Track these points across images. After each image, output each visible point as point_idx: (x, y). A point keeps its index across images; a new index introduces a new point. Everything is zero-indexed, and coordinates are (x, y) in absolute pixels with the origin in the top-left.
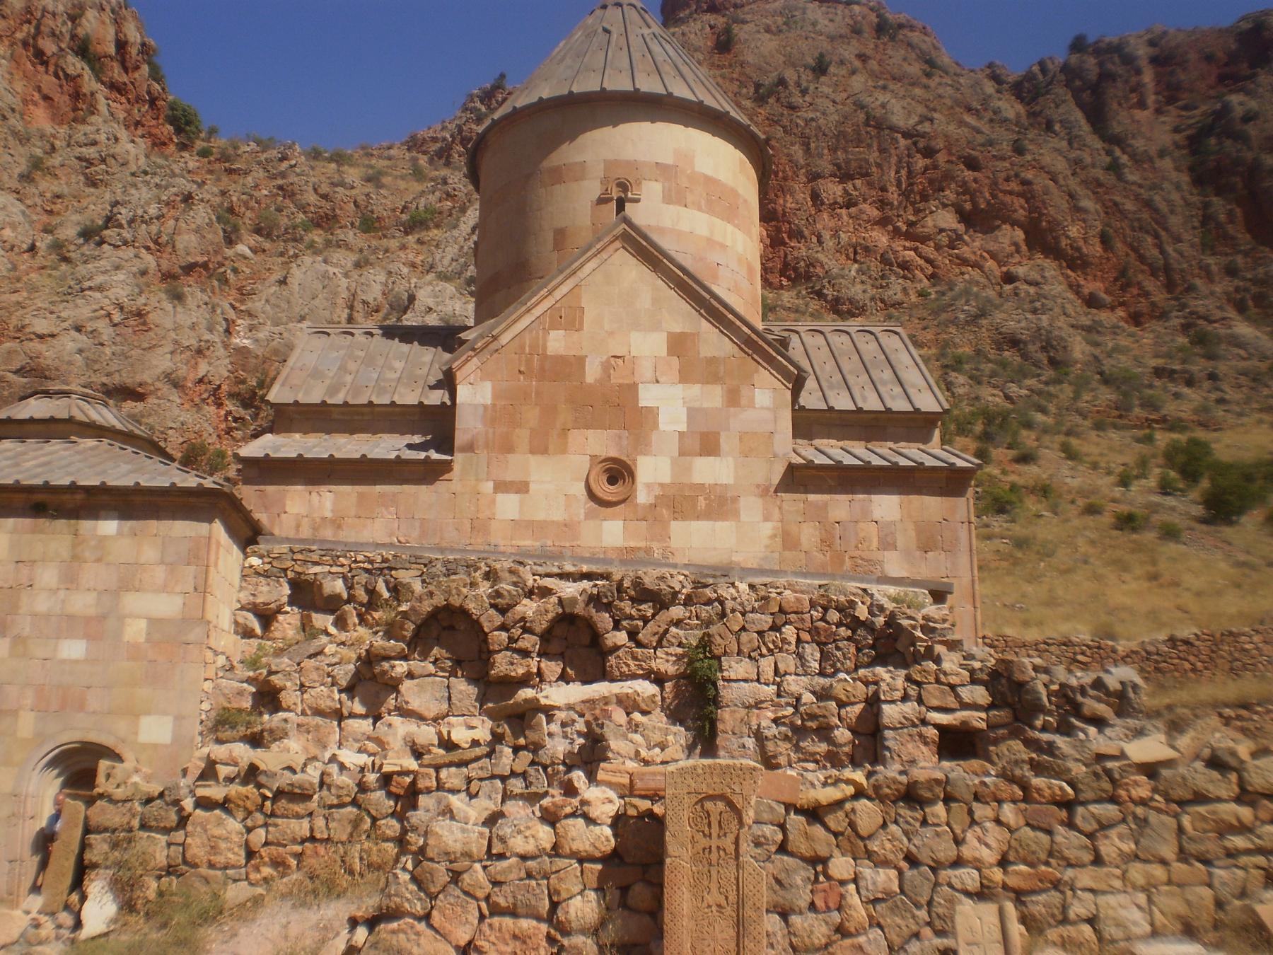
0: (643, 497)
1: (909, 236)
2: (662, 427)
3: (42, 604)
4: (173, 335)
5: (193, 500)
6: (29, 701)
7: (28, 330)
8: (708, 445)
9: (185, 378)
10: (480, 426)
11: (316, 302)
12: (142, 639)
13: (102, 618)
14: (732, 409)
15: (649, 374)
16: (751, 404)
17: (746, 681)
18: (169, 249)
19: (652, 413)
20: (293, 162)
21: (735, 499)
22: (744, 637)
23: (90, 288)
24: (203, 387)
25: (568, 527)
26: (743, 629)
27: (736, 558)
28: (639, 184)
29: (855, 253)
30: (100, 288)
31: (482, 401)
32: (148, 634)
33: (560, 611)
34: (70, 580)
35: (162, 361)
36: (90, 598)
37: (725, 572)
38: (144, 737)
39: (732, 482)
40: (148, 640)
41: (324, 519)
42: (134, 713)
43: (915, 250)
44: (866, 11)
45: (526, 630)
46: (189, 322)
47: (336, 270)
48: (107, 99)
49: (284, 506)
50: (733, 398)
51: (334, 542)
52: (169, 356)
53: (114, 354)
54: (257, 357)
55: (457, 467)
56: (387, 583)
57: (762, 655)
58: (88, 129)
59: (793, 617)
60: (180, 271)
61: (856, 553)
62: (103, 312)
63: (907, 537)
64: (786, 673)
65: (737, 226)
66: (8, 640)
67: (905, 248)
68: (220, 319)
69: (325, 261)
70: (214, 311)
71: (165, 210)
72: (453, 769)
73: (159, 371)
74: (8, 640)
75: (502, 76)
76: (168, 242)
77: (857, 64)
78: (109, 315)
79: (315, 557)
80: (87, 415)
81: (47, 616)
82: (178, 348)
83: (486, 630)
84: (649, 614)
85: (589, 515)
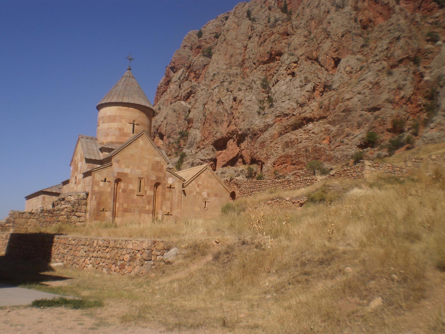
4: (388, 87)
7: (344, 99)
9: (394, 99)
18: (392, 58)
23: (362, 80)
24: (403, 100)
30: (364, 79)
35: (385, 96)
46: (393, 80)
52: (387, 94)
54: (431, 82)
58: (391, 20)
60: (397, 63)
62: (366, 86)
70: (409, 72)
71: (389, 46)
73: (384, 99)
76: (391, 56)
78: (368, 86)
82: (390, 90)
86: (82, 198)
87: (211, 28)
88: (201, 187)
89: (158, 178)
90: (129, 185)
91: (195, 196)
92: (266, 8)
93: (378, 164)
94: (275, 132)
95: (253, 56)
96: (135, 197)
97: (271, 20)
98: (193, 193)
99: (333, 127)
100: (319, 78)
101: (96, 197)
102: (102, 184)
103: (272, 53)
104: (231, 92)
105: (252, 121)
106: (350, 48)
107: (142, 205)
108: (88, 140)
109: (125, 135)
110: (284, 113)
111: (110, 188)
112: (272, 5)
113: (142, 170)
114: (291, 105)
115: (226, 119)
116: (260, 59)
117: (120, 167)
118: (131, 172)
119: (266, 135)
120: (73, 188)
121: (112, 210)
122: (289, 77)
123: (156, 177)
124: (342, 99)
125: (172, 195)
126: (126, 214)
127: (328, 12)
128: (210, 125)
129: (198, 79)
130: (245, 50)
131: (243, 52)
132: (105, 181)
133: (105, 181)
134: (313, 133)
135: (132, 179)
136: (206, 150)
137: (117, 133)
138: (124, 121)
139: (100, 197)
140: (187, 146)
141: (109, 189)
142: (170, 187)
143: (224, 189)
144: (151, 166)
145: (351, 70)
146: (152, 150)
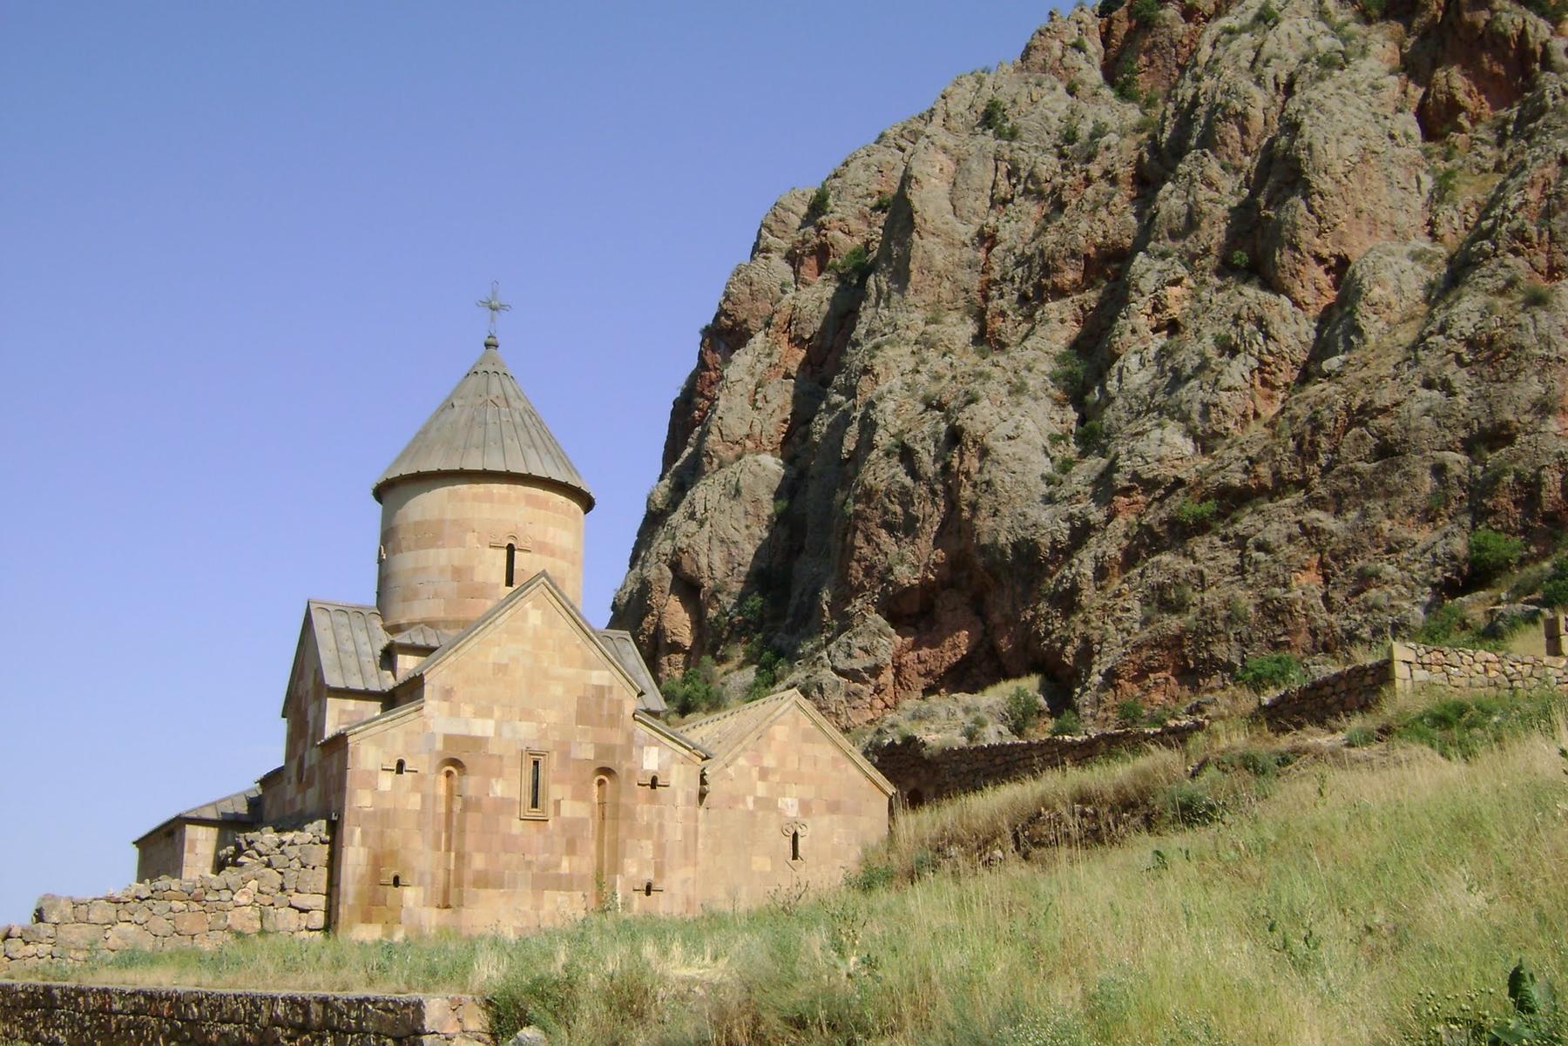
53: (1470, 399)
65: (443, 546)
78: (1459, 359)
86: (317, 840)
87: (862, 176)
88: (775, 778)
89: (604, 750)
90: (493, 781)
91: (752, 814)
92: (1061, 88)
93: (1440, 656)
94: (1113, 551)
96: (517, 827)
97: (1080, 133)
98: (744, 802)
99: (1332, 520)
100: (1267, 336)
101: (364, 834)
102: (386, 781)
103: (1087, 257)
104: (940, 407)
105: (1024, 515)
106: (1384, 216)
107: (543, 857)
108: (344, 619)
109: (479, 591)
110: (1145, 476)
111: (418, 797)
113: (541, 723)
115: (929, 509)
116: (1044, 281)
117: (454, 713)
118: (498, 733)
119: (1084, 563)
120: (292, 802)
121: (428, 879)
122: (1160, 340)
123: (596, 746)
124: (1362, 410)
125: (660, 814)
126: (483, 893)
128: (868, 540)
129: (821, 366)
130: (989, 250)
131: (981, 255)
132: (400, 766)
133: (400, 766)
134: (1261, 547)
135: (500, 757)
136: (856, 635)
137: (449, 586)
138: (471, 539)
139: (382, 833)
140: (788, 621)
141: (415, 802)
142: (654, 784)
143: (866, 783)
144: (572, 708)
145: (1393, 299)
146: (578, 646)
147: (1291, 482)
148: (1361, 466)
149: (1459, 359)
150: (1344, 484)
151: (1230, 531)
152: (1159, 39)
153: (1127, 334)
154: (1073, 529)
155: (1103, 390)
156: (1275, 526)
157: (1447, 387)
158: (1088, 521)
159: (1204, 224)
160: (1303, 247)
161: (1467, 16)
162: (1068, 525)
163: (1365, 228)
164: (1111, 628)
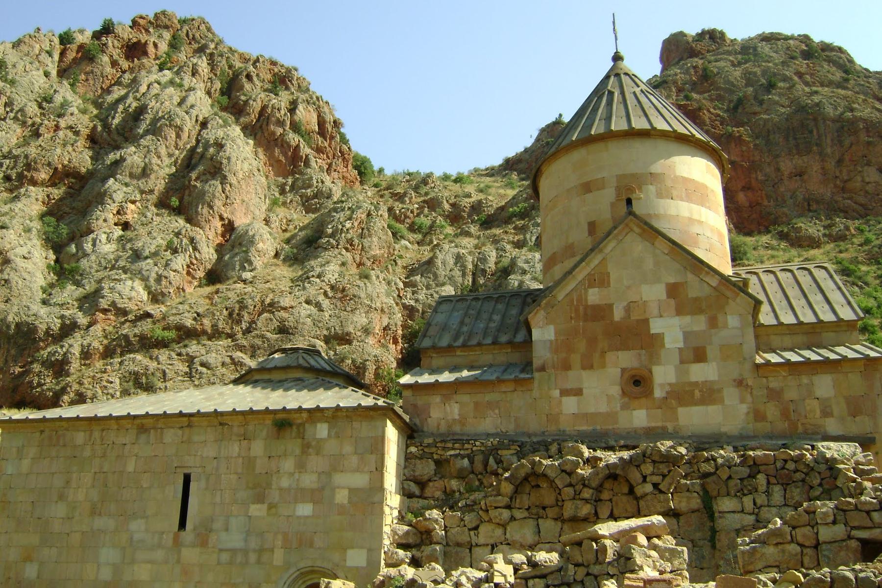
0: (658, 393)
1: (843, 190)
2: (667, 346)
3: (285, 483)
5: (371, 413)
6: (279, 543)
8: (700, 356)
10: (548, 355)
11: (453, 273)
12: (346, 502)
13: (322, 489)
14: (713, 330)
15: (656, 312)
16: (725, 326)
17: (734, 512)
19: (659, 337)
20: (433, 185)
21: (720, 391)
22: (731, 483)
23: (313, 276)
25: (611, 416)
26: (730, 477)
27: (724, 429)
28: (640, 189)
29: (809, 205)
31: (549, 338)
32: (350, 498)
33: (607, 472)
34: (301, 466)
35: (360, 319)
36: (314, 477)
37: (717, 440)
38: (349, 563)
39: (717, 378)
40: (349, 502)
41: (454, 420)
42: (343, 549)
43: (850, 198)
44: (797, 43)
45: (584, 485)
47: (464, 251)
48: (315, 158)
49: (429, 413)
50: (713, 323)
51: (462, 435)
53: (330, 316)
55: (536, 383)
56: (495, 459)
57: (745, 495)
59: (762, 468)
61: (804, 421)
63: (839, 408)
64: (761, 506)
66: (265, 507)
67: (844, 198)
68: (394, 288)
69: (456, 246)
72: (537, 580)
74: (265, 506)
75: (560, 115)
77: (796, 78)
79: (450, 445)
80: (309, 363)
81: (288, 490)
83: (560, 486)
84: (666, 471)
85: (624, 407)
92: (41, 72)
94: (96, 344)
95: (8, 161)
100: (195, 249)
103: (56, 169)
106: (252, 209)
110: (119, 306)
112: (49, 69)
114: (138, 293)
116: (25, 173)
122: (118, 232)
124: (271, 304)
127: (204, 125)
134: (203, 365)
147: (223, 332)
148: (269, 335)
149: (325, 294)
150: (258, 342)
151: (184, 351)
152: (95, 70)
153: (101, 222)
154: (63, 326)
155: (79, 247)
156: (214, 355)
157: (318, 306)
158: (77, 322)
159: (153, 176)
160: (215, 208)
161: (272, 127)
162: (60, 321)
163: (244, 211)
164: (100, 391)
